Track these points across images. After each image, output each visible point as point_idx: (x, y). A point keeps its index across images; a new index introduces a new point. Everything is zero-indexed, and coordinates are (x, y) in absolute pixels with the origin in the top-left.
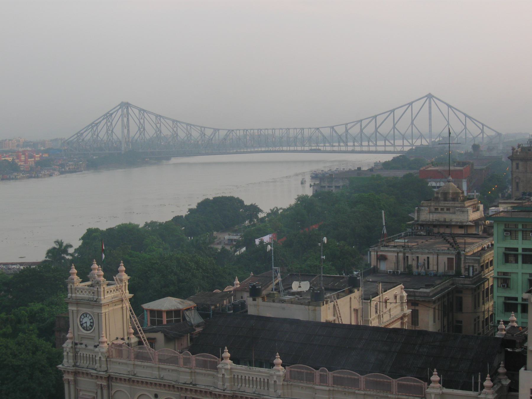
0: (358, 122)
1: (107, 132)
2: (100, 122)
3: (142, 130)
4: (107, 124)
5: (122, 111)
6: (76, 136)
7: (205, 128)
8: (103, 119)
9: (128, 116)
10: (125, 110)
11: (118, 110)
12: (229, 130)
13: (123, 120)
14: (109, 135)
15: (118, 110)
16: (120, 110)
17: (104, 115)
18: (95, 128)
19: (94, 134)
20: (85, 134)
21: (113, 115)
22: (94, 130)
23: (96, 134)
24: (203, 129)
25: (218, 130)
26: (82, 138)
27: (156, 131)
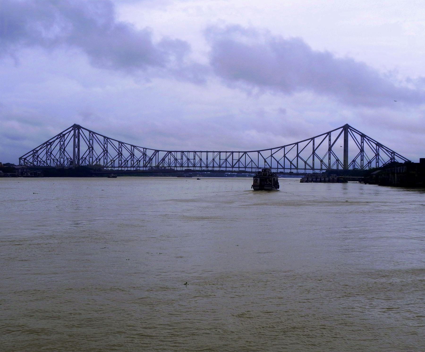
0: (282, 147)
1: (60, 149)
2: (54, 141)
3: (91, 149)
4: (60, 143)
5: (75, 132)
6: (32, 152)
7: (146, 149)
8: (57, 139)
9: (79, 137)
10: (77, 131)
11: (70, 131)
12: (168, 151)
13: (74, 140)
14: (62, 152)
15: (70, 131)
16: (73, 132)
17: (58, 135)
18: (49, 147)
19: (48, 152)
20: (39, 152)
21: (66, 136)
22: (49, 148)
23: (50, 151)
24: (145, 149)
25: (158, 151)
26: (37, 155)
27: (104, 150)
